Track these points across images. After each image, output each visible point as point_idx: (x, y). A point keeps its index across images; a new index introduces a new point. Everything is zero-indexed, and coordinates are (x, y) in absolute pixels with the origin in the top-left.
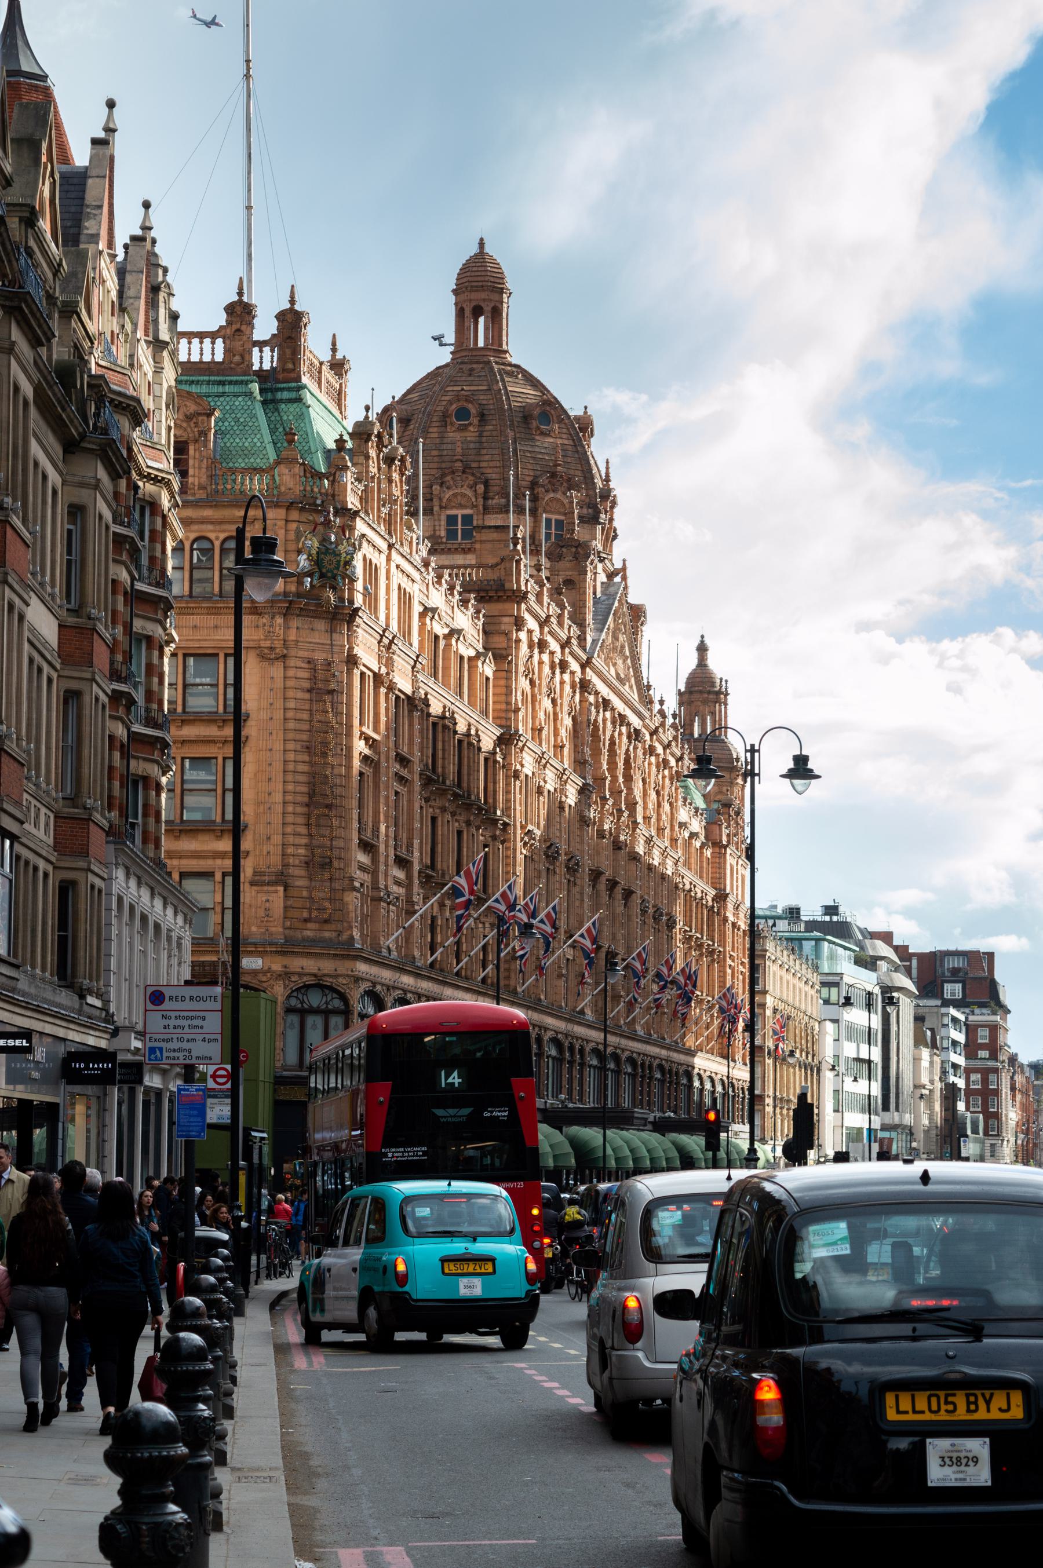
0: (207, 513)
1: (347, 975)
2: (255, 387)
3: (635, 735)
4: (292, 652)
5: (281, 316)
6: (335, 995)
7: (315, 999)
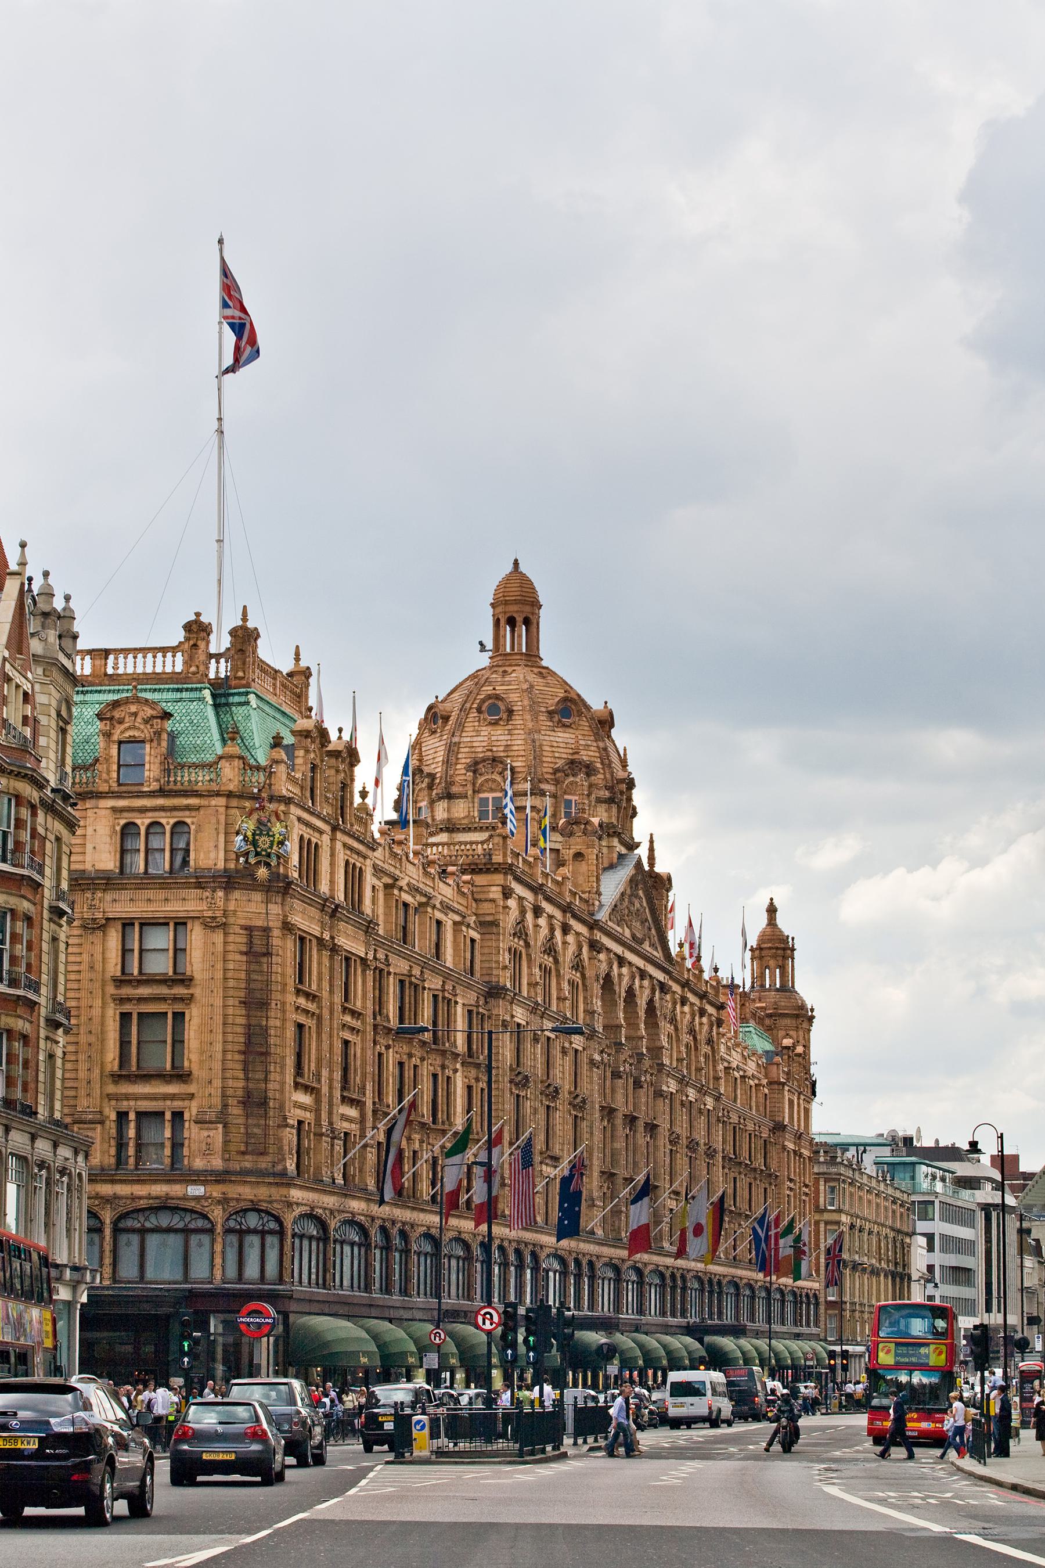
0: (160, 802)
2: (207, 693)
3: (663, 988)
4: (231, 920)
5: (233, 633)
6: (270, 1218)
7: (253, 1221)
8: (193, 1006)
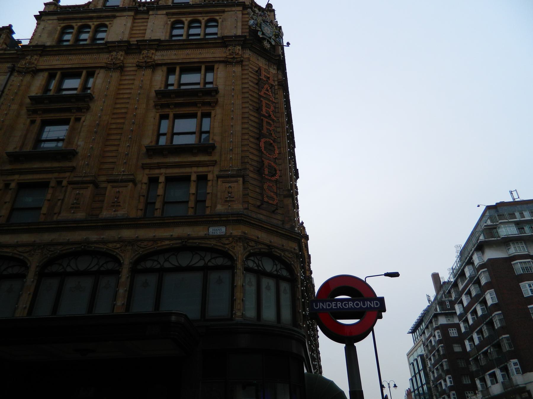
1: (292, 252)
6: (282, 267)
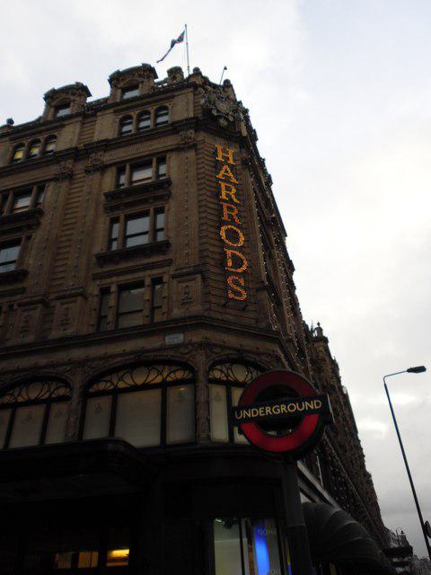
8: (171, 200)
